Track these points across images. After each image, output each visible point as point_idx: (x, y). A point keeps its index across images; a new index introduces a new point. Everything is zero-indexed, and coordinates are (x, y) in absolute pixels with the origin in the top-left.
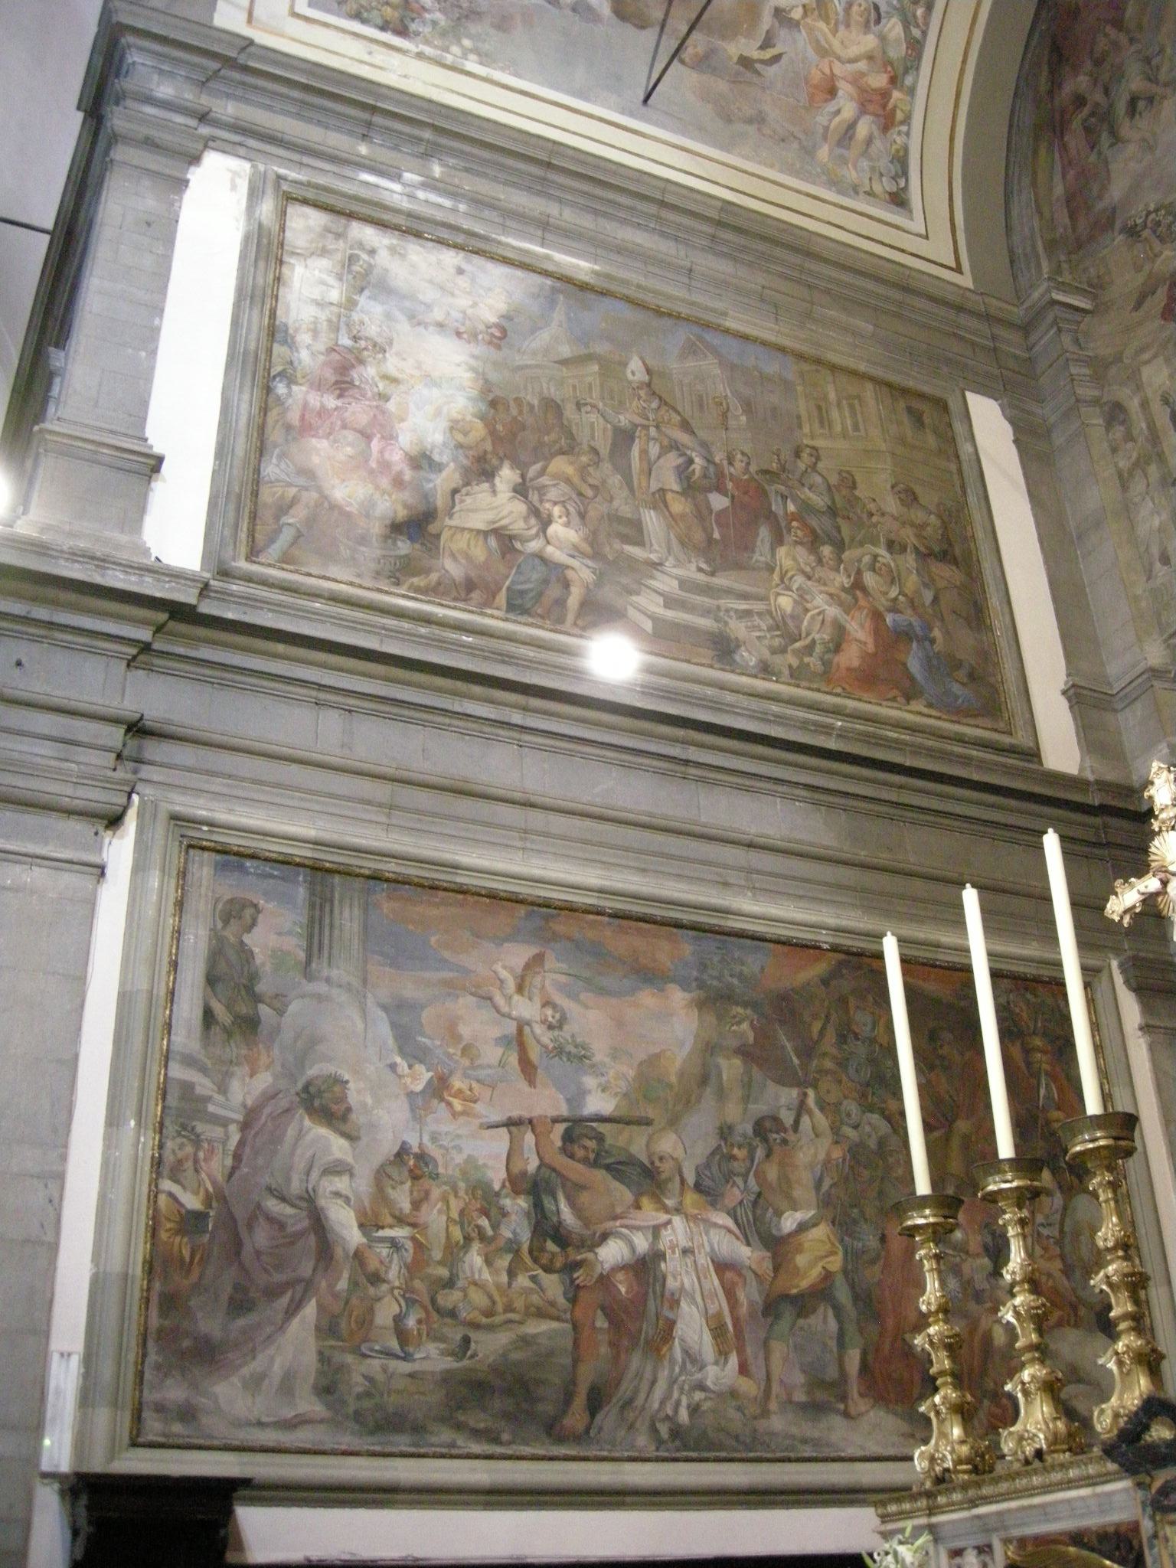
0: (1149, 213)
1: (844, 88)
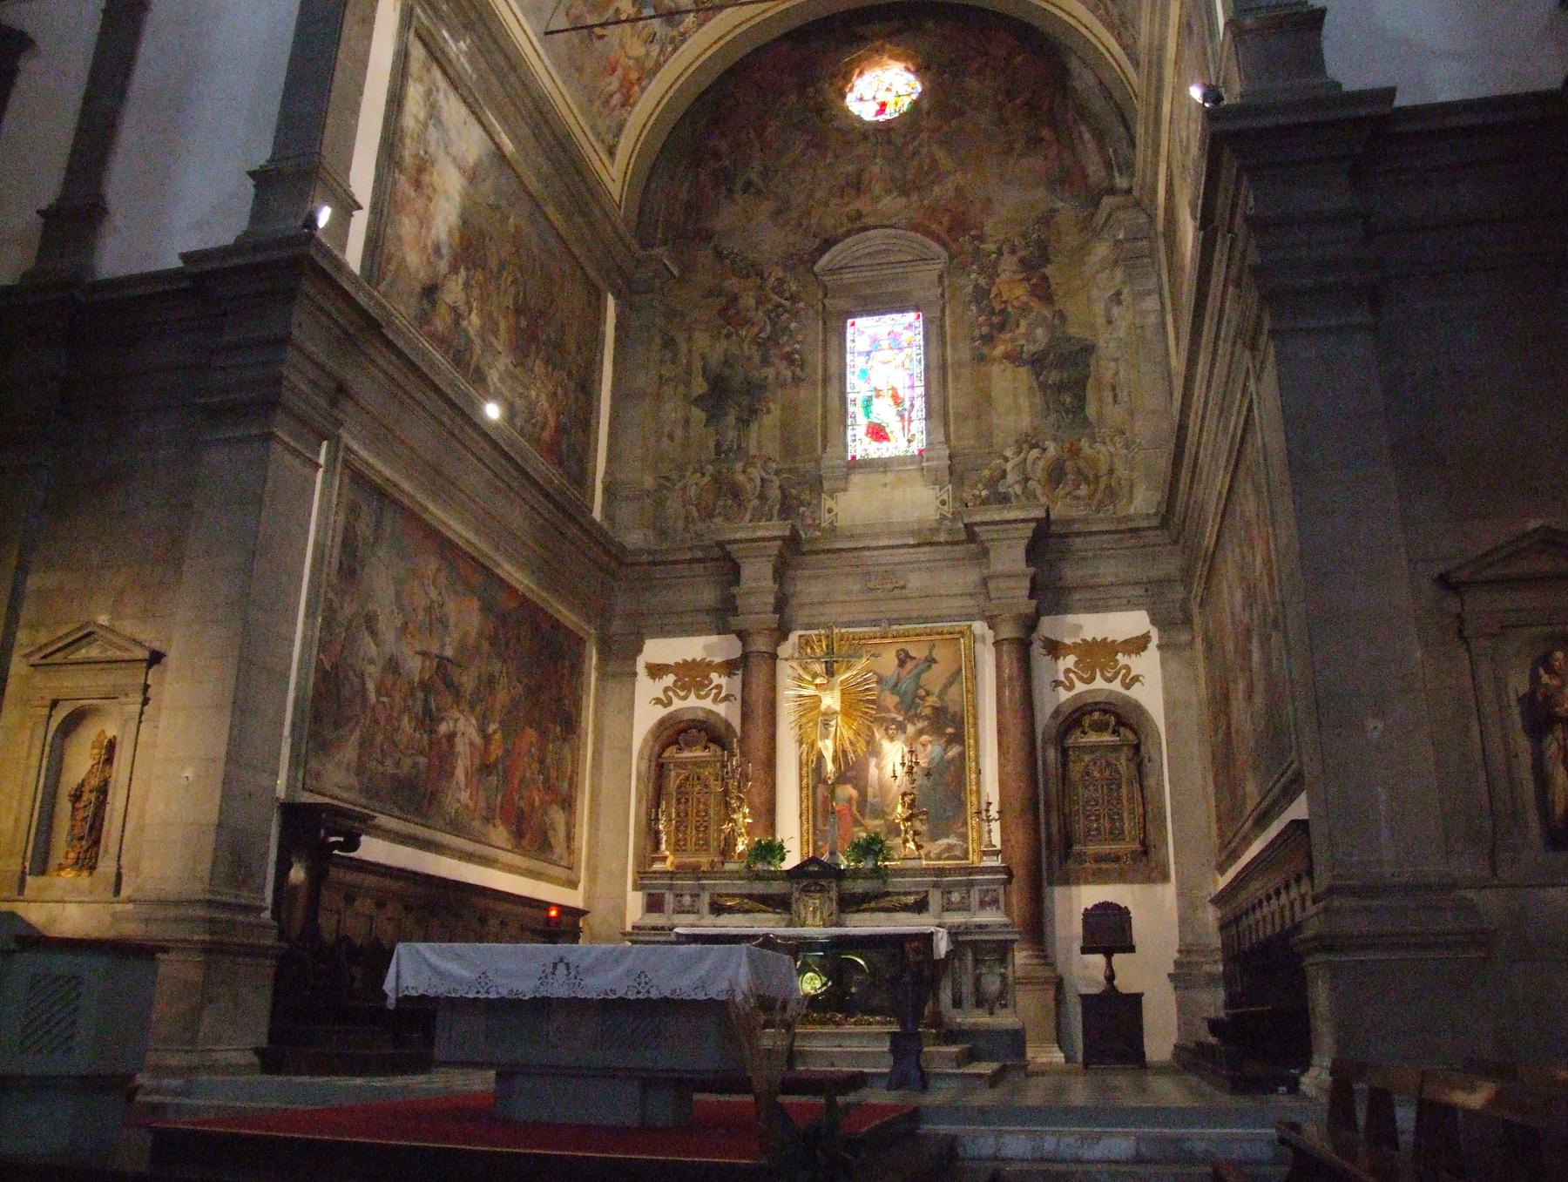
0: (732, 253)
1: (619, 71)
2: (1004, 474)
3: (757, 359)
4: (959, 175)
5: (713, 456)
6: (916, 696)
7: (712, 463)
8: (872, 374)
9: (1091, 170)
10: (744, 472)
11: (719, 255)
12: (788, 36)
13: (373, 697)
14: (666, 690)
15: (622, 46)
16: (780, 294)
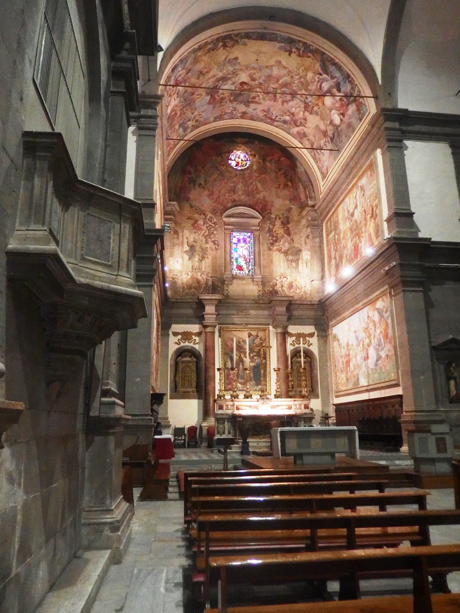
2: (276, 285)
5: (191, 270)
8: (238, 250)
11: (191, 206)
14: (179, 340)
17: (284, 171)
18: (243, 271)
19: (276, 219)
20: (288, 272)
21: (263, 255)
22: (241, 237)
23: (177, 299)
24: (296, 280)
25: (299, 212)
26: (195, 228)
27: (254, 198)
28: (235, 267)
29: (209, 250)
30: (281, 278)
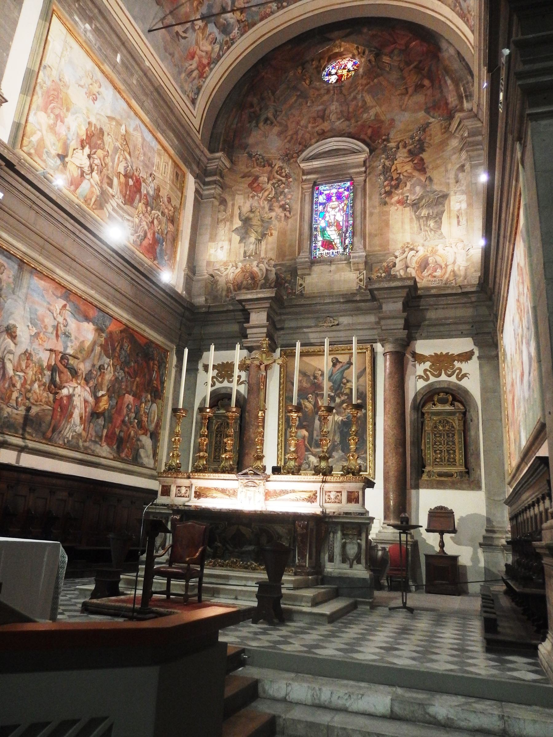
3: (267, 209)
4: (378, 108)
5: (242, 258)
6: (341, 382)
7: (241, 262)
9: (450, 100)
10: (257, 266)
11: (250, 156)
12: (290, 41)
13: (10, 372)
15: (197, 43)
16: (280, 175)
17: (415, 64)
18: (334, 249)
19: (398, 148)
20: (419, 239)
21: (371, 214)
22: (334, 191)
23: (209, 307)
24: (434, 252)
25: (445, 128)
26: (253, 189)
27: (357, 122)
28: (320, 244)
29: (275, 222)
30: (404, 252)
